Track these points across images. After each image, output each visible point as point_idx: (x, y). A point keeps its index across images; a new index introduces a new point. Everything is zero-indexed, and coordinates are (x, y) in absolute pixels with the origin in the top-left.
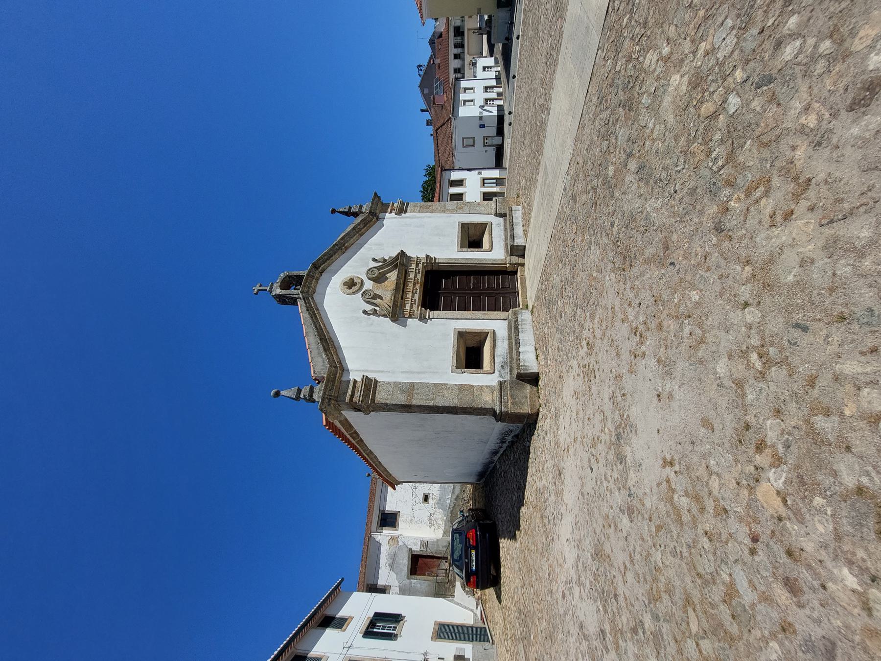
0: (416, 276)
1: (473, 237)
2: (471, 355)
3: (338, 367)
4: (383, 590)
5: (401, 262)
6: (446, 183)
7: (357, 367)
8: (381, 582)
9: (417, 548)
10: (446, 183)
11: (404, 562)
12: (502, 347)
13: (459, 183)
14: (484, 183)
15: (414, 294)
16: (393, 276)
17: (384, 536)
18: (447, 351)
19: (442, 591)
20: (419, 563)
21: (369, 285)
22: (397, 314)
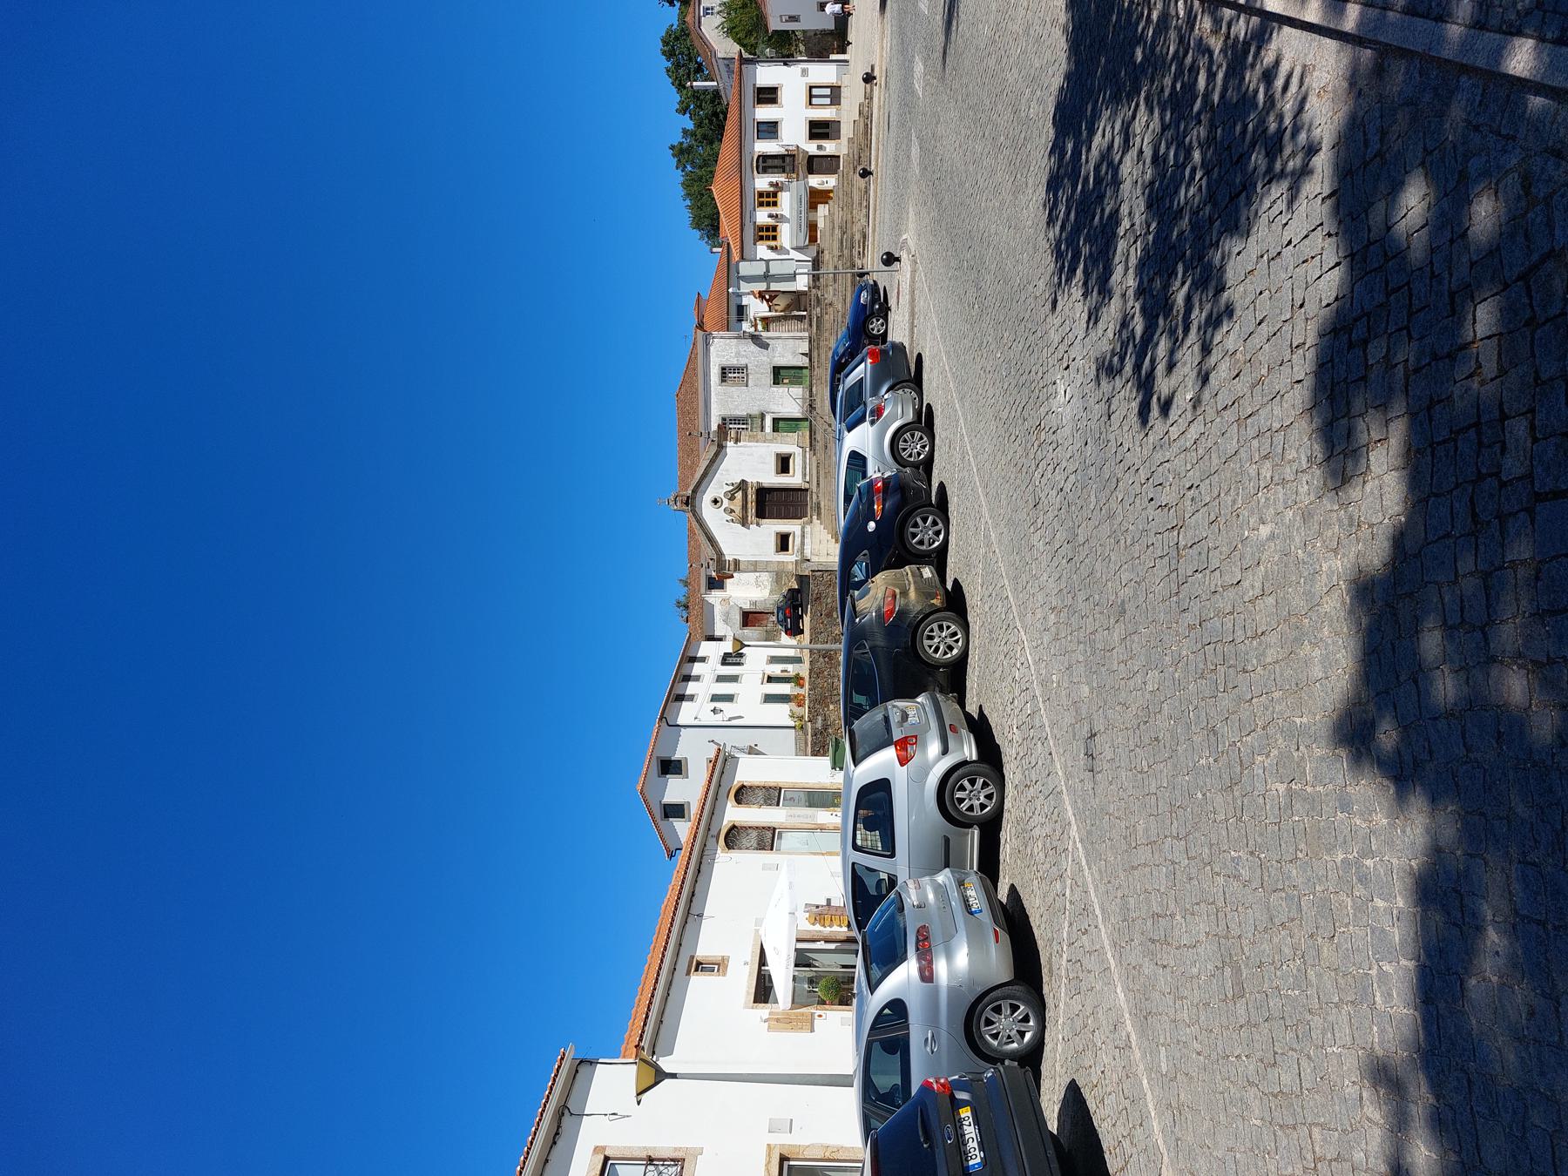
0: (752, 497)
1: (784, 464)
2: (783, 542)
3: (720, 554)
4: (720, 639)
5: (742, 486)
6: (749, 95)
7: (729, 556)
8: (718, 633)
9: (747, 607)
10: (751, 131)
11: (737, 618)
12: (798, 540)
13: (768, 95)
14: (811, 96)
15: (752, 509)
16: (739, 495)
17: (714, 597)
18: (772, 543)
19: (770, 636)
20: (749, 618)
21: (726, 503)
22: (744, 522)
